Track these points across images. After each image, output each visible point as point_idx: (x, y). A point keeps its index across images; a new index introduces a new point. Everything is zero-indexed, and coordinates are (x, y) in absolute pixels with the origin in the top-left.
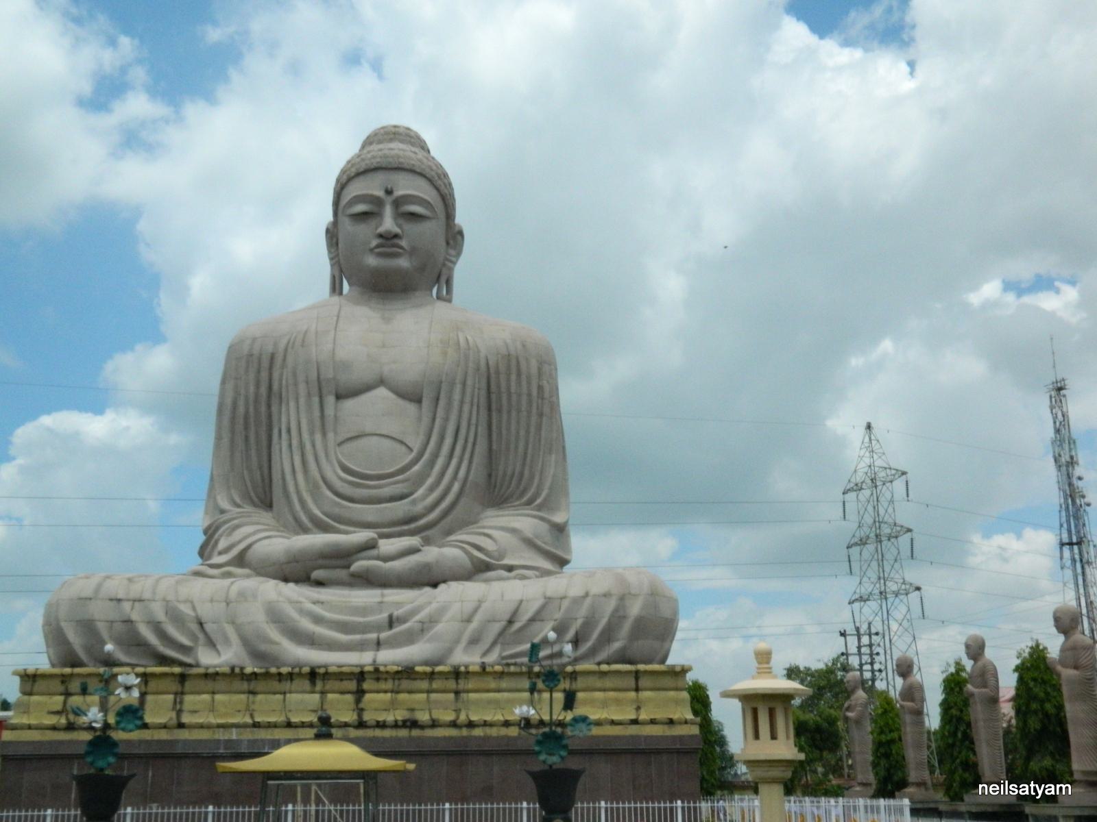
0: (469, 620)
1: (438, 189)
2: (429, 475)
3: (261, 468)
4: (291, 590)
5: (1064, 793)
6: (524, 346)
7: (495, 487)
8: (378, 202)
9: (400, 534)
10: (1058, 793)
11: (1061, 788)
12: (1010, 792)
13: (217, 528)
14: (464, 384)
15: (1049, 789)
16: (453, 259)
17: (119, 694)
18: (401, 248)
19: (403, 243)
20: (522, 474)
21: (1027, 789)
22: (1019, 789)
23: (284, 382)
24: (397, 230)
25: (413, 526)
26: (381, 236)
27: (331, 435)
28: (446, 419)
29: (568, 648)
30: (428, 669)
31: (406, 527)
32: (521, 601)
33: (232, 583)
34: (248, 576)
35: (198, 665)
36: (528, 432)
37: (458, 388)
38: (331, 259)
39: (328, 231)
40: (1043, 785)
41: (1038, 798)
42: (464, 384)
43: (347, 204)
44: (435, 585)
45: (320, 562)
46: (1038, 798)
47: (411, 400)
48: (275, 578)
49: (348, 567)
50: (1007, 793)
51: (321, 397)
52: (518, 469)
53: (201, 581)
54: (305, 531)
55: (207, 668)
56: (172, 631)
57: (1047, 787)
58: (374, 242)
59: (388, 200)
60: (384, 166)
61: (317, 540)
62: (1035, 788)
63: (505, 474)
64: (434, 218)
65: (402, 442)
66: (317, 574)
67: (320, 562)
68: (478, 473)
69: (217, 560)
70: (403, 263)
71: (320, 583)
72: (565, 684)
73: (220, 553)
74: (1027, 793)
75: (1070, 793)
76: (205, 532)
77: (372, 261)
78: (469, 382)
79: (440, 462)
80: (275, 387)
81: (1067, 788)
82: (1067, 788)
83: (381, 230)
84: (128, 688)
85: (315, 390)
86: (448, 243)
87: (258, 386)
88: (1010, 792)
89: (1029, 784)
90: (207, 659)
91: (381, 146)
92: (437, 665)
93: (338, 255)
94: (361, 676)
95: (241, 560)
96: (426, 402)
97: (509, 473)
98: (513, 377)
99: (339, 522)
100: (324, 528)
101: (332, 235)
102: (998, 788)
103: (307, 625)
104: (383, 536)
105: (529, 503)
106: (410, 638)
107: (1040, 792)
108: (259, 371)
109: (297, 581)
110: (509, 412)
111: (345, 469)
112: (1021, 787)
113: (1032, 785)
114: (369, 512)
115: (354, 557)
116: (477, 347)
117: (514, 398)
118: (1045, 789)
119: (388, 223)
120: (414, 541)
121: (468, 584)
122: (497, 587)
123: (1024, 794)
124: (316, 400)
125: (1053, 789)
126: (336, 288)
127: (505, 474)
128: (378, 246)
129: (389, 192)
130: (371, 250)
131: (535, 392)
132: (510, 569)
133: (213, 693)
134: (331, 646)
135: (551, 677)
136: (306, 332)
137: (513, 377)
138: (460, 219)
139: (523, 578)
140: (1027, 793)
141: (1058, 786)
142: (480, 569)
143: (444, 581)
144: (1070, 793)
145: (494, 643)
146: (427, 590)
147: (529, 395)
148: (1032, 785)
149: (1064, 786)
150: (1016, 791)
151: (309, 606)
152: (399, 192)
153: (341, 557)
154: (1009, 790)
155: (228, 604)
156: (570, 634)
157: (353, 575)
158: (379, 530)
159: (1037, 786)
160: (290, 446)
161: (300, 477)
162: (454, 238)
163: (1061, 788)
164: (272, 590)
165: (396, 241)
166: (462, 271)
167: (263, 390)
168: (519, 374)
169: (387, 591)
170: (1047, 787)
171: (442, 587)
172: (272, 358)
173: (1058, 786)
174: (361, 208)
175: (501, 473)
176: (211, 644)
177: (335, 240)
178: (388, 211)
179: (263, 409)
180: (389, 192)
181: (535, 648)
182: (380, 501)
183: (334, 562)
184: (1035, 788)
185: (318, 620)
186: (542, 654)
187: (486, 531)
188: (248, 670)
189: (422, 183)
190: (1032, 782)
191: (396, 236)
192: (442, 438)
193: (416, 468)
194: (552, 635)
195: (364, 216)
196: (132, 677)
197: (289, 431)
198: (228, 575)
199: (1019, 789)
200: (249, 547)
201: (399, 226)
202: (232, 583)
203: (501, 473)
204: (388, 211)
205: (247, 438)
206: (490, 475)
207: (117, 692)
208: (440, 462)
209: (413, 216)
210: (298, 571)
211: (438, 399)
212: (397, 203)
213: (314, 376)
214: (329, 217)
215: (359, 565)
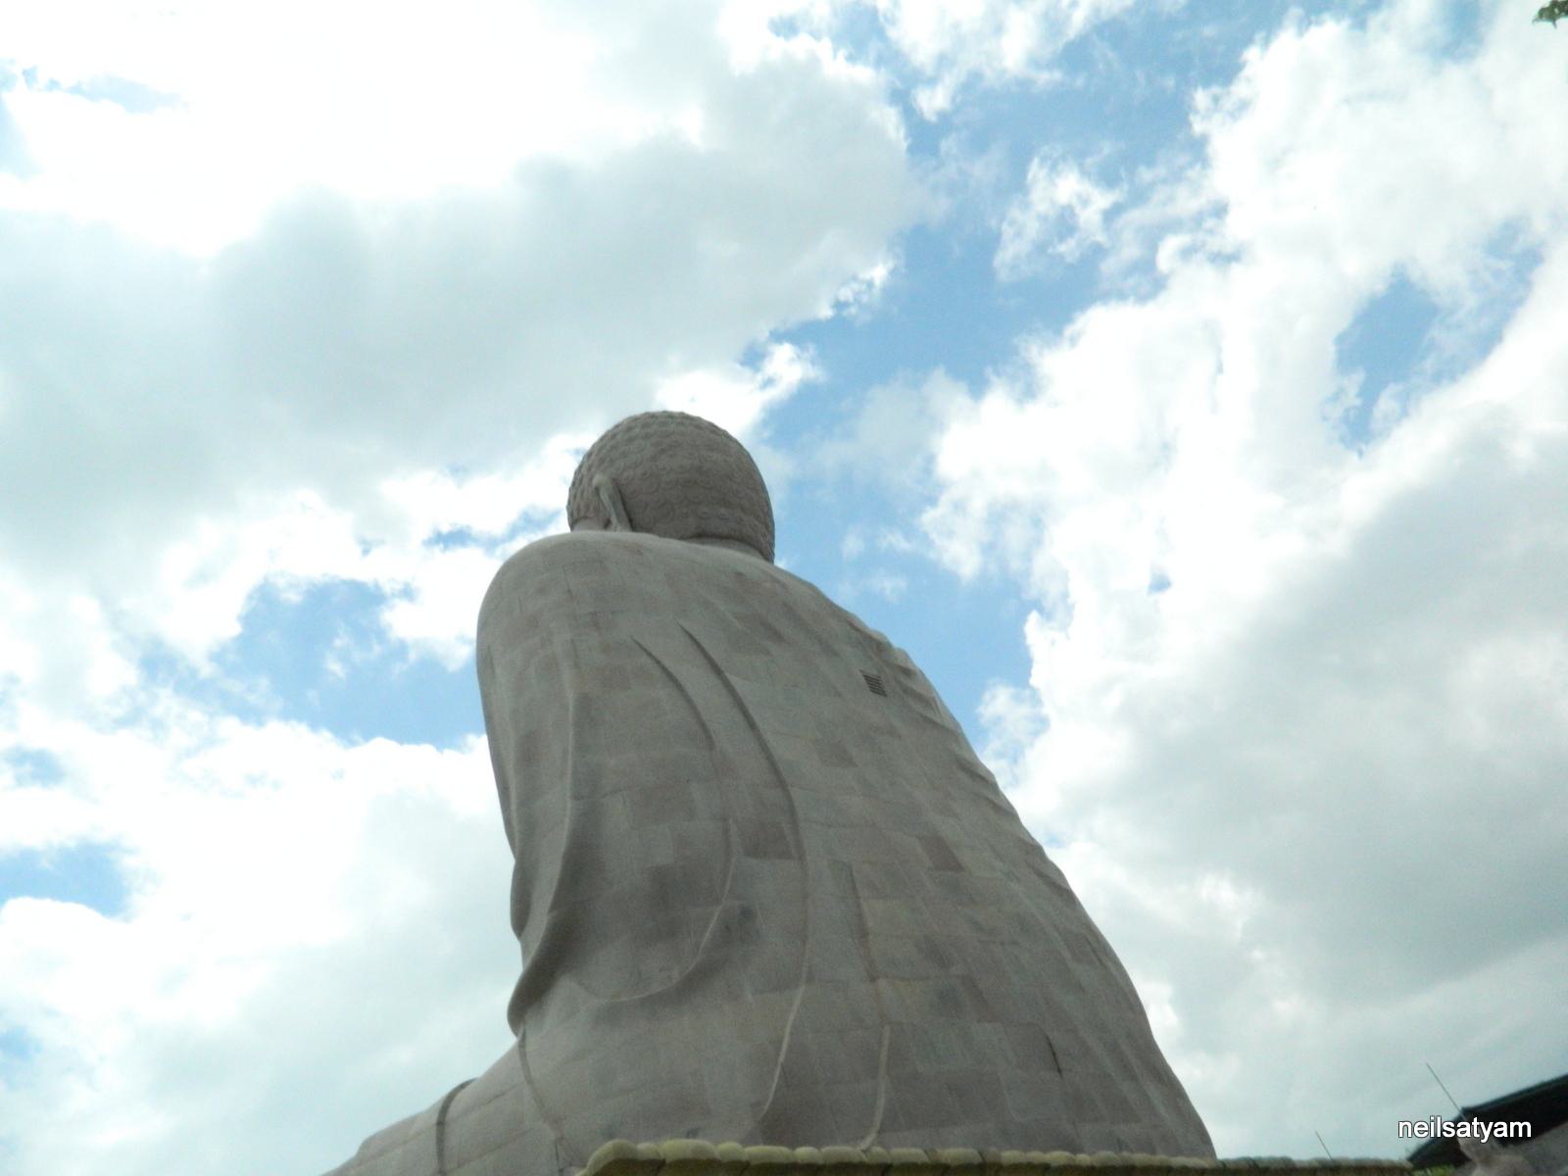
5: (1520, 1135)
10: (1512, 1135)
11: (1516, 1128)
12: (1444, 1133)
15: (1500, 1129)
21: (1468, 1129)
22: (1456, 1129)
40: (1491, 1124)
41: (1483, 1141)
46: (1483, 1141)
50: (1439, 1136)
57: (1496, 1125)
62: (1479, 1126)
74: (1468, 1134)
75: (1529, 1135)
81: (1525, 1127)
82: (1525, 1127)
88: (1444, 1133)
89: (1471, 1122)
102: (1426, 1128)
107: (1487, 1134)
112: (1459, 1125)
113: (1475, 1123)
118: (1493, 1128)
123: (1464, 1135)
125: (1505, 1129)
140: (1468, 1134)
141: (1512, 1125)
144: (1529, 1135)
148: (1475, 1123)
149: (1521, 1125)
150: (1453, 1131)
154: (1442, 1130)
159: (1482, 1124)
163: (1516, 1128)
170: (1496, 1125)
173: (1512, 1125)
184: (1479, 1126)
190: (1475, 1119)
199: (1456, 1129)
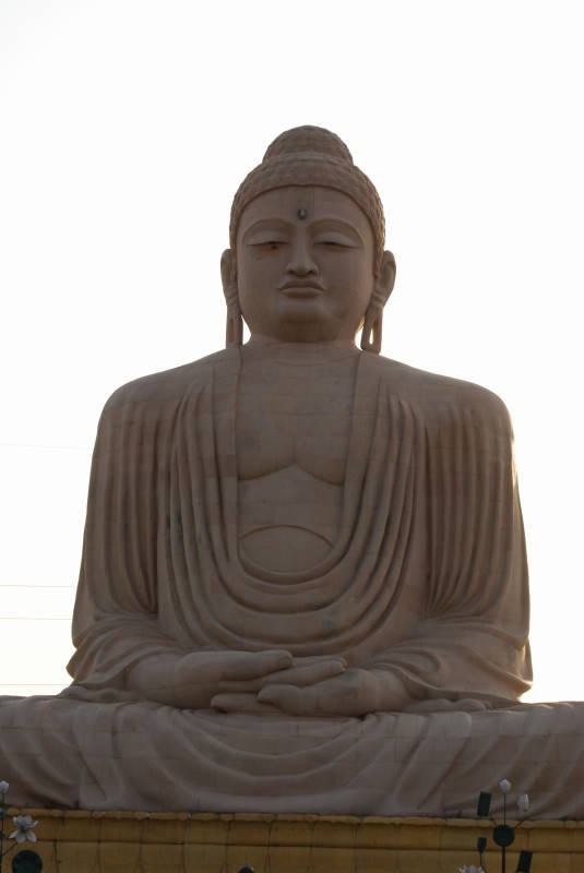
0: (405, 762)
1: (362, 209)
2: (354, 578)
3: (143, 565)
4: (187, 721)
6: (473, 412)
7: (435, 592)
8: (288, 229)
9: (320, 652)
13: (91, 639)
14: (398, 464)
16: (382, 297)
17: (14, 839)
18: (316, 287)
19: (320, 281)
20: (470, 576)
23: (172, 461)
24: (309, 265)
25: (332, 641)
26: (291, 272)
27: (231, 528)
28: (376, 508)
29: (526, 798)
30: (356, 820)
31: (325, 643)
32: (468, 740)
33: (118, 709)
34: (135, 701)
35: (77, 807)
36: (478, 521)
37: (392, 467)
38: (226, 296)
39: (223, 262)
42: (398, 464)
43: (250, 229)
44: (362, 717)
45: (223, 685)
47: (331, 483)
48: (167, 705)
49: (256, 692)
51: (219, 479)
52: (465, 569)
53: (81, 707)
54: (198, 644)
55: (92, 811)
56: (44, 762)
58: (288, 279)
59: (302, 226)
60: (296, 183)
61: (216, 659)
63: (448, 576)
64: (357, 248)
65: (322, 538)
66: (218, 700)
67: (223, 685)
68: (414, 576)
69: (92, 678)
70: (322, 307)
71: (221, 711)
72: (520, 842)
73: (97, 671)
76: (76, 643)
77: (283, 305)
78: (407, 459)
79: (371, 559)
80: (162, 464)
83: (293, 266)
84: (23, 830)
85: (210, 469)
86: (375, 277)
87: (140, 460)
90: (89, 799)
91: (291, 156)
92: (364, 815)
93: (237, 293)
94: (270, 822)
95: (125, 684)
96: (351, 488)
97: (454, 575)
98: (460, 452)
99: (242, 635)
100: (225, 644)
101: (229, 264)
103: (206, 761)
104: (297, 654)
105: (477, 614)
106: (332, 782)
108: (141, 444)
109: (194, 707)
110: (454, 494)
111: (247, 569)
114: (281, 625)
115: (264, 679)
116: (413, 415)
117: (460, 479)
119: (303, 259)
120: (338, 662)
121: (403, 717)
122: (441, 719)
124: (212, 483)
127: (448, 576)
128: (287, 286)
130: (280, 289)
131: (488, 471)
132: (454, 697)
133: (99, 841)
134: (240, 789)
135: (504, 836)
136: (200, 395)
137: (460, 452)
138: (389, 245)
139: (471, 710)
142: (418, 697)
143: (373, 712)
145: (435, 790)
146: (353, 721)
147: (480, 475)
151: (211, 739)
152: (318, 217)
153: (248, 679)
155: (114, 733)
156: (527, 784)
157: (264, 702)
158: (294, 646)
160: (181, 538)
161: (192, 578)
162: (384, 269)
164: (163, 717)
165: (313, 279)
166: (391, 312)
167: (148, 467)
168: (466, 449)
169: (304, 723)
171: (371, 720)
172: (158, 425)
174: (269, 236)
175: (443, 574)
176: (94, 781)
177: (233, 273)
178: (301, 244)
179: (147, 492)
181: (485, 799)
182: (293, 611)
183: (238, 685)
185: (221, 757)
186: (494, 804)
187: (428, 649)
188: (140, 815)
189: (348, 205)
191: (311, 272)
192: (370, 533)
193: (337, 569)
194: (506, 783)
195: (273, 245)
196: (28, 820)
197: (179, 519)
198: (108, 699)
200: (137, 662)
201: (315, 260)
202: (118, 709)
203: (443, 574)
204: (301, 244)
205: (126, 528)
206: (428, 577)
207: (12, 836)
208: (371, 559)
209: (330, 245)
210: (196, 700)
211: (364, 481)
212: (313, 230)
213: (208, 453)
214: (228, 246)
215: (266, 693)
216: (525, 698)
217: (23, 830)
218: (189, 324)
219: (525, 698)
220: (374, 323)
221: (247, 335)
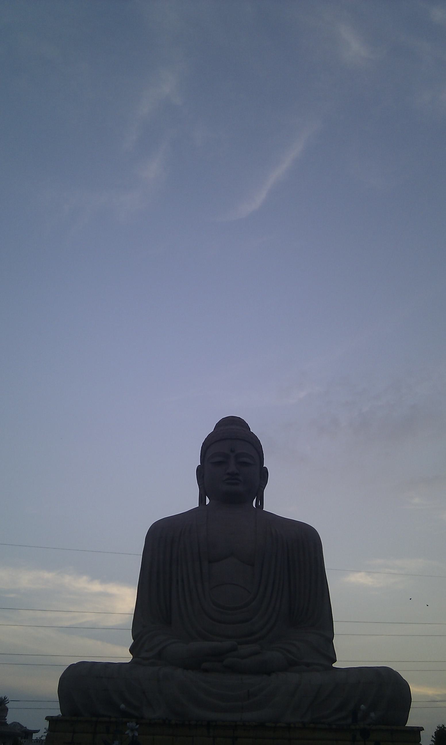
26: (228, 474)
44: (269, 674)
71: (206, 671)
76: (133, 639)
101: (200, 472)
126: (202, 500)
129: (232, 451)
162: (264, 474)
166: (267, 492)
180: (232, 451)
195: (219, 463)
196: (134, 724)
209: (245, 464)
216: (334, 665)
217: (132, 730)
218: (183, 496)
219: (334, 665)
220: (261, 499)
221: (208, 501)
